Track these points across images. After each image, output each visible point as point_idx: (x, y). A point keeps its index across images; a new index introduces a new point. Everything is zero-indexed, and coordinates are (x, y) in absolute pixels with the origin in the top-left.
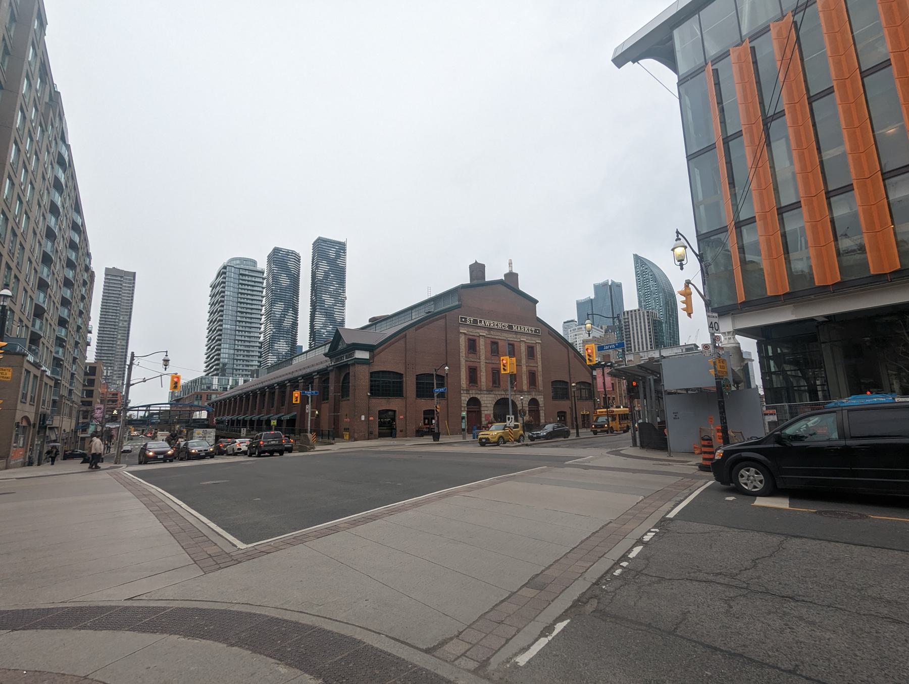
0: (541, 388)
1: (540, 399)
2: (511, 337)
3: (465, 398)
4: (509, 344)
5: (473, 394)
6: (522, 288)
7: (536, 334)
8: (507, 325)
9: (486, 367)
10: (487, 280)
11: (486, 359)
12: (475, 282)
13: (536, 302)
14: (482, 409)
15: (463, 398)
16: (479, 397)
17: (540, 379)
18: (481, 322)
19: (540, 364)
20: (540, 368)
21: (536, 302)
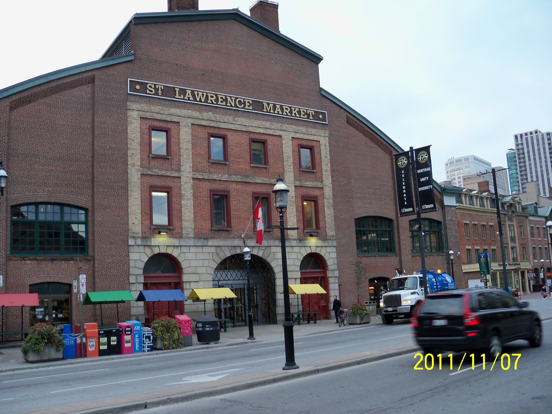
0: (331, 232)
1: (330, 256)
2: (257, 126)
3: (139, 258)
4: (254, 141)
5: (162, 242)
6: (287, 27)
7: (318, 120)
8: (249, 100)
9: (195, 188)
10: (200, 8)
11: (195, 169)
12: (176, 12)
13: (316, 59)
14: (185, 278)
15: (132, 256)
16: (175, 253)
17: (328, 213)
18: (183, 92)
19: (327, 181)
20: (328, 192)
21: (316, 59)
